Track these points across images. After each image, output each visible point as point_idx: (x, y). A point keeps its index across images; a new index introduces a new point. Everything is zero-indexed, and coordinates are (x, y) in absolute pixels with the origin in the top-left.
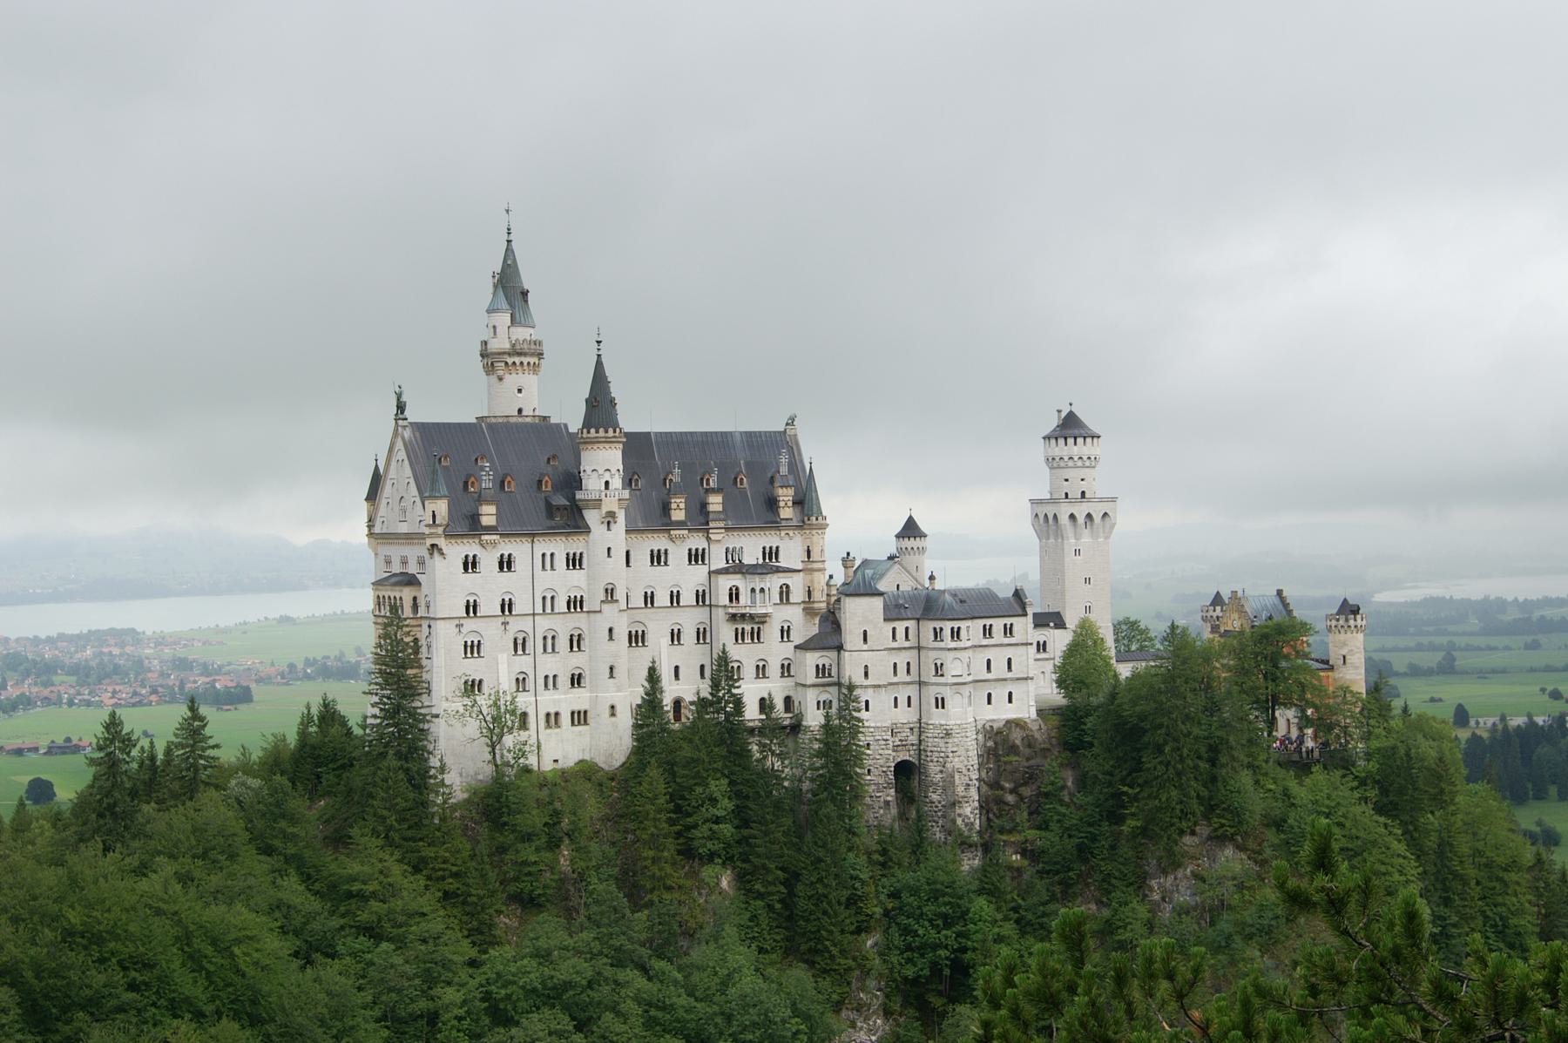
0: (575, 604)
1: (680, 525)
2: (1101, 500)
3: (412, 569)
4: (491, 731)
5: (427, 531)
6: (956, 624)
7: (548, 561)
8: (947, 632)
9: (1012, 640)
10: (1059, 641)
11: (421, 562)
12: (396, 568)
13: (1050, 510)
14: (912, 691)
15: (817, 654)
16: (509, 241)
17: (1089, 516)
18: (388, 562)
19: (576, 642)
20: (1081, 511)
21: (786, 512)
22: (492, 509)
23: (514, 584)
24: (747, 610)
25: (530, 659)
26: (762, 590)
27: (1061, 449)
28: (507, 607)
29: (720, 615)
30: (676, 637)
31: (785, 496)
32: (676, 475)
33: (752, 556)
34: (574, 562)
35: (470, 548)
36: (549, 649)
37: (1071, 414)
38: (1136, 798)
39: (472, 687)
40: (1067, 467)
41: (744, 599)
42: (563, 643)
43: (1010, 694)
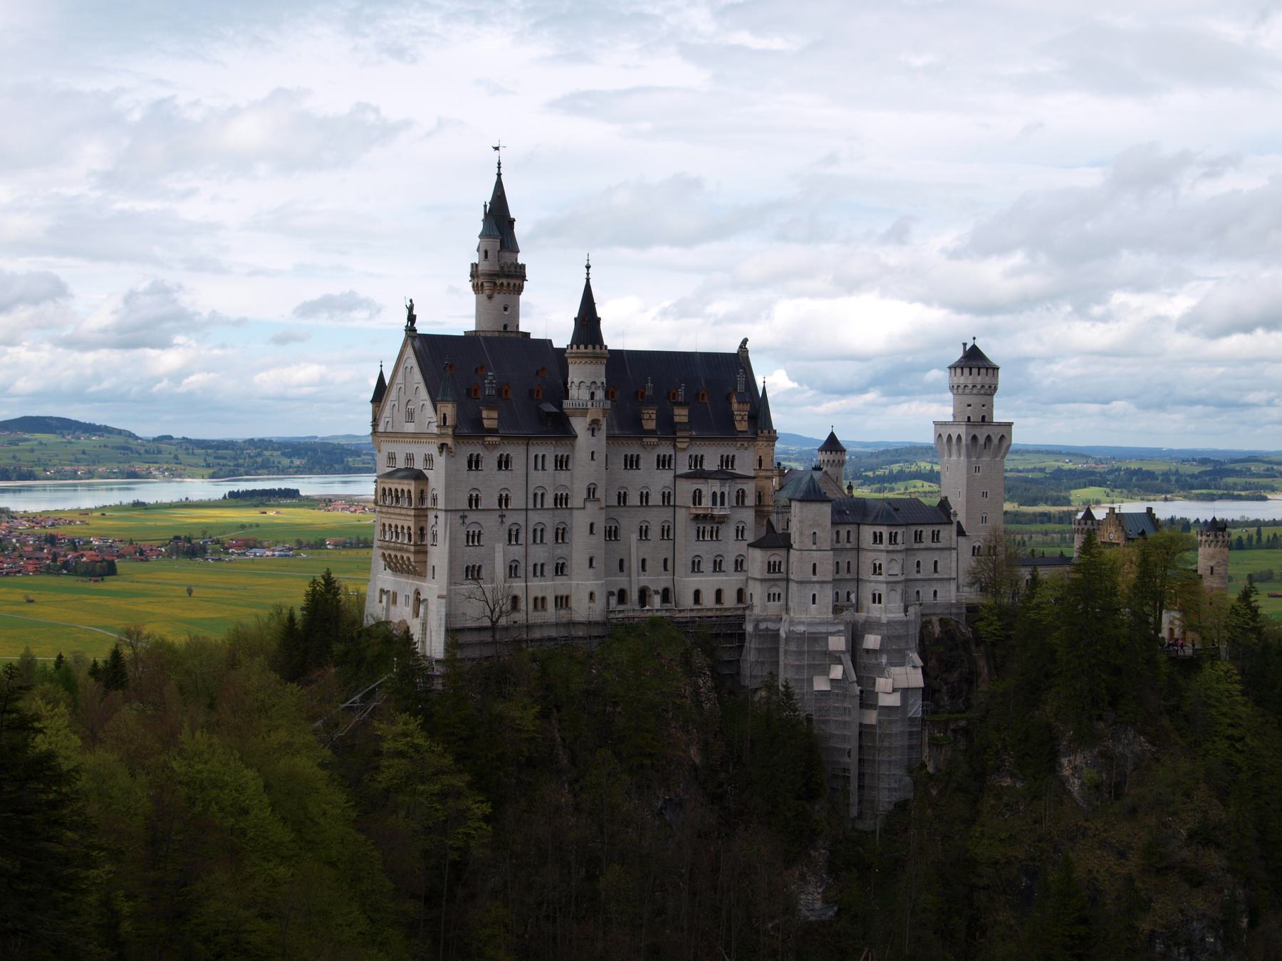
1: (651, 433)
2: (1000, 424)
3: (419, 465)
4: (492, 612)
5: (435, 430)
7: (539, 463)
8: (886, 537)
9: (939, 545)
10: (965, 546)
11: (429, 459)
12: (401, 464)
13: (955, 432)
14: (851, 587)
15: (769, 553)
17: (989, 438)
18: (392, 457)
19: (561, 534)
20: (982, 433)
21: (742, 426)
22: (495, 415)
23: (512, 481)
26: (723, 494)
28: (504, 501)
29: (682, 515)
30: (644, 533)
31: (739, 411)
32: (649, 389)
33: (711, 464)
34: (562, 463)
35: (476, 449)
36: (538, 540)
37: (974, 348)
39: (473, 573)
40: (971, 394)
41: (706, 502)
42: (549, 536)
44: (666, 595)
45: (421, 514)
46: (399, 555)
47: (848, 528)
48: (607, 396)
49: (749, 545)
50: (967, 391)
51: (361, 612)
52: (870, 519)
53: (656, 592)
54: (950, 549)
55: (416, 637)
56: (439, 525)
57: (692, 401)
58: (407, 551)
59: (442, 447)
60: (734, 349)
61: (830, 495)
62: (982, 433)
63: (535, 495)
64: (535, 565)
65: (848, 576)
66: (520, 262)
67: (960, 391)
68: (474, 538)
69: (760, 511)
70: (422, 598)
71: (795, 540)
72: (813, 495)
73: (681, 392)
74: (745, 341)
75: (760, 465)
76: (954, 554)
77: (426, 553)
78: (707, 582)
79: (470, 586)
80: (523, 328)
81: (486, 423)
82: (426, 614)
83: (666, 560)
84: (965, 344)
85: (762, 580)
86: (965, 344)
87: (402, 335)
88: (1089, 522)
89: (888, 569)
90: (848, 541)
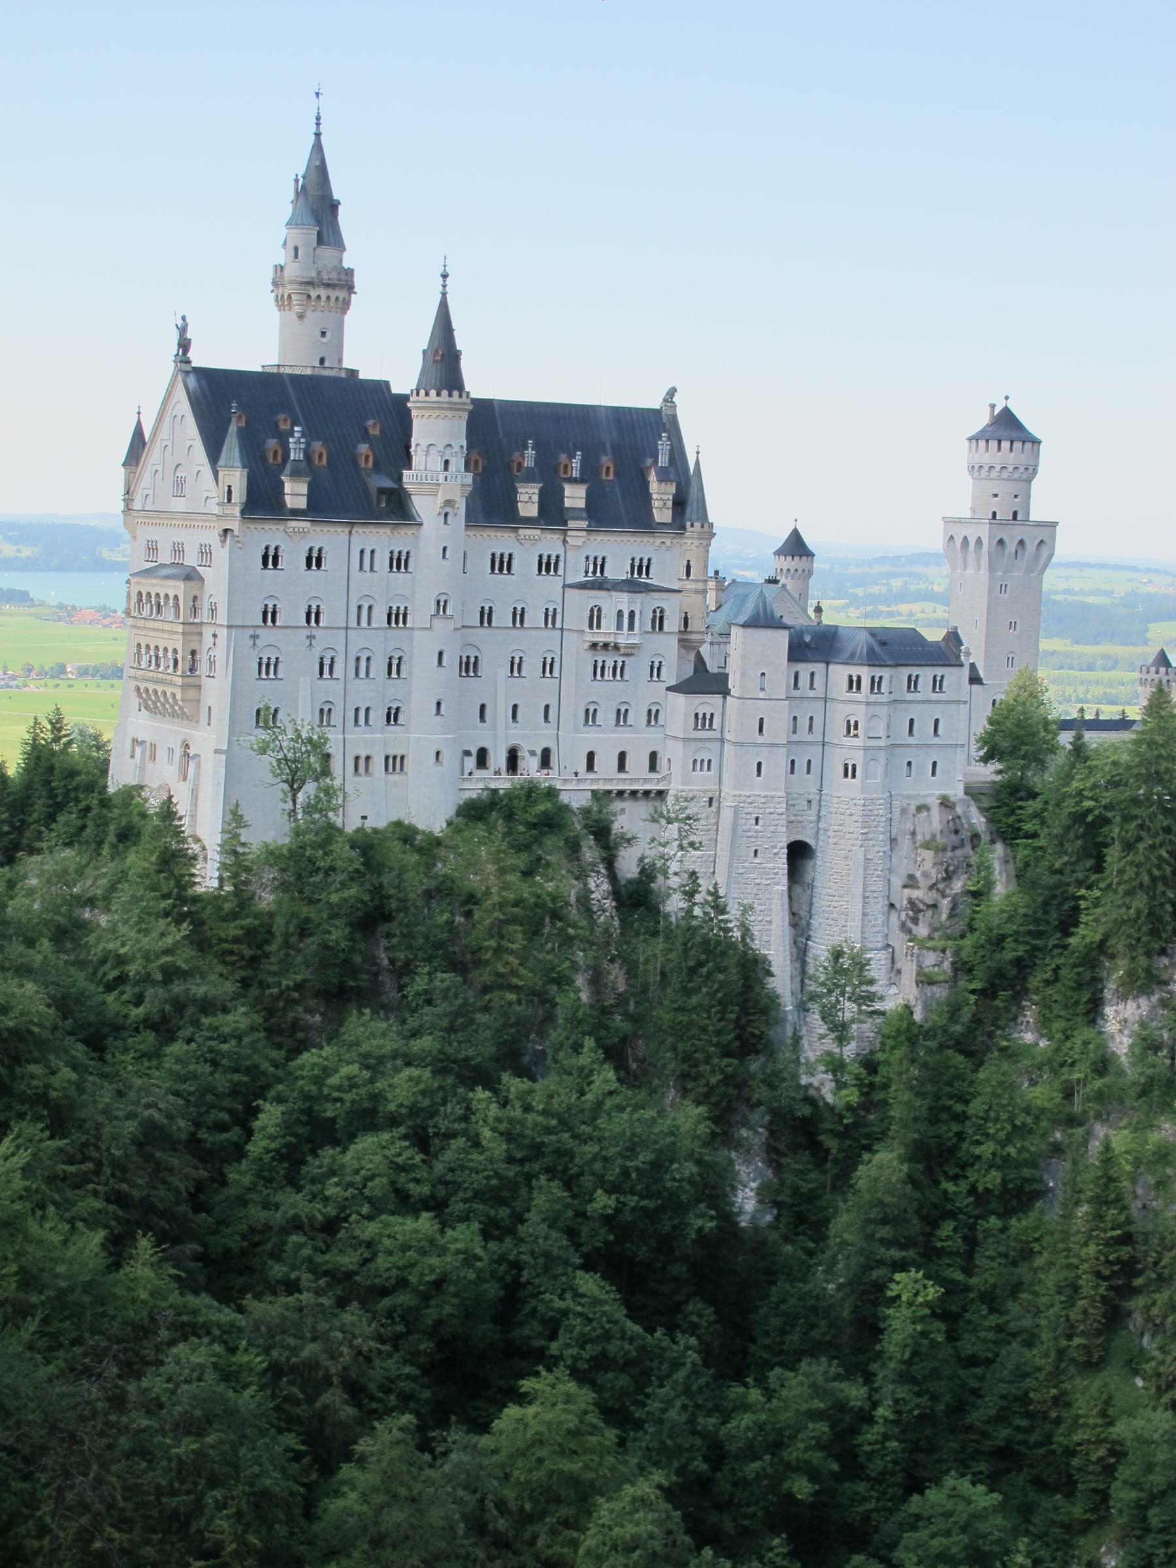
0: (396, 617)
1: (529, 522)
2: (1039, 524)
3: (191, 559)
5: (216, 510)
6: (877, 672)
7: (367, 559)
8: (866, 683)
11: (205, 552)
12: (165, 557)
14: (814, 753)
15: (698, 699)
16: (318, 135)
17: (1021, 542)
18: (152, 548)
19: (394, 667)
20: (1012, 536)
21: (662, 513)
24: (611, 639)
25: (340, 686)
26: (632, 614)
27: (990, 455)
28: (313, 616)
30: (516, 666)
31: (660, 494)
32: (529, 458)
33: (617, 571)
34: (399, 562)
36: (362, 674)
38: (1097, 903)
39: (266, 718)
40: (999, 478)
42: (379, 668)
43: (935, 764)
44: (545, 759)
45: (192, 630)
46: (160, 689)
47: (812, 667)
48: (467, 468)
49: (668, 689)
50: (994, 474)
51: (105, 772)
52: (845, 655)
53: (533, 753)
54: (958, 702)
55: (182, 808)
56: (218, 648)
57: (589, 475)
58: (172, 684)
59: (226, 531)
60: (656, 405)
61: (787, 621)
62: (1012, 536)
63: (360, 607)
64: (357, 710)
65: (810, 738)
66: (346, 265)
67: (984, 473)
68: (268, 667)
69: (685, 643)
70: (192, 752)
71: (734, 683)
72: (763, 620)
73: (576, 463)
74: (672, 392)
75: (688, 574)
76: (964, 709)
77: (200, 686)
78: (606, 742)
79: (264, 735)
80: (345, 365)
81: (290, 502)
82: (197, 775)
83: (547, 707)
84: (993, 406)
85: (686, 740)
86: (993, 406)
87: (167, 367)
88: (1162, 670)
89: (868, 729)
90: (812, 687)
